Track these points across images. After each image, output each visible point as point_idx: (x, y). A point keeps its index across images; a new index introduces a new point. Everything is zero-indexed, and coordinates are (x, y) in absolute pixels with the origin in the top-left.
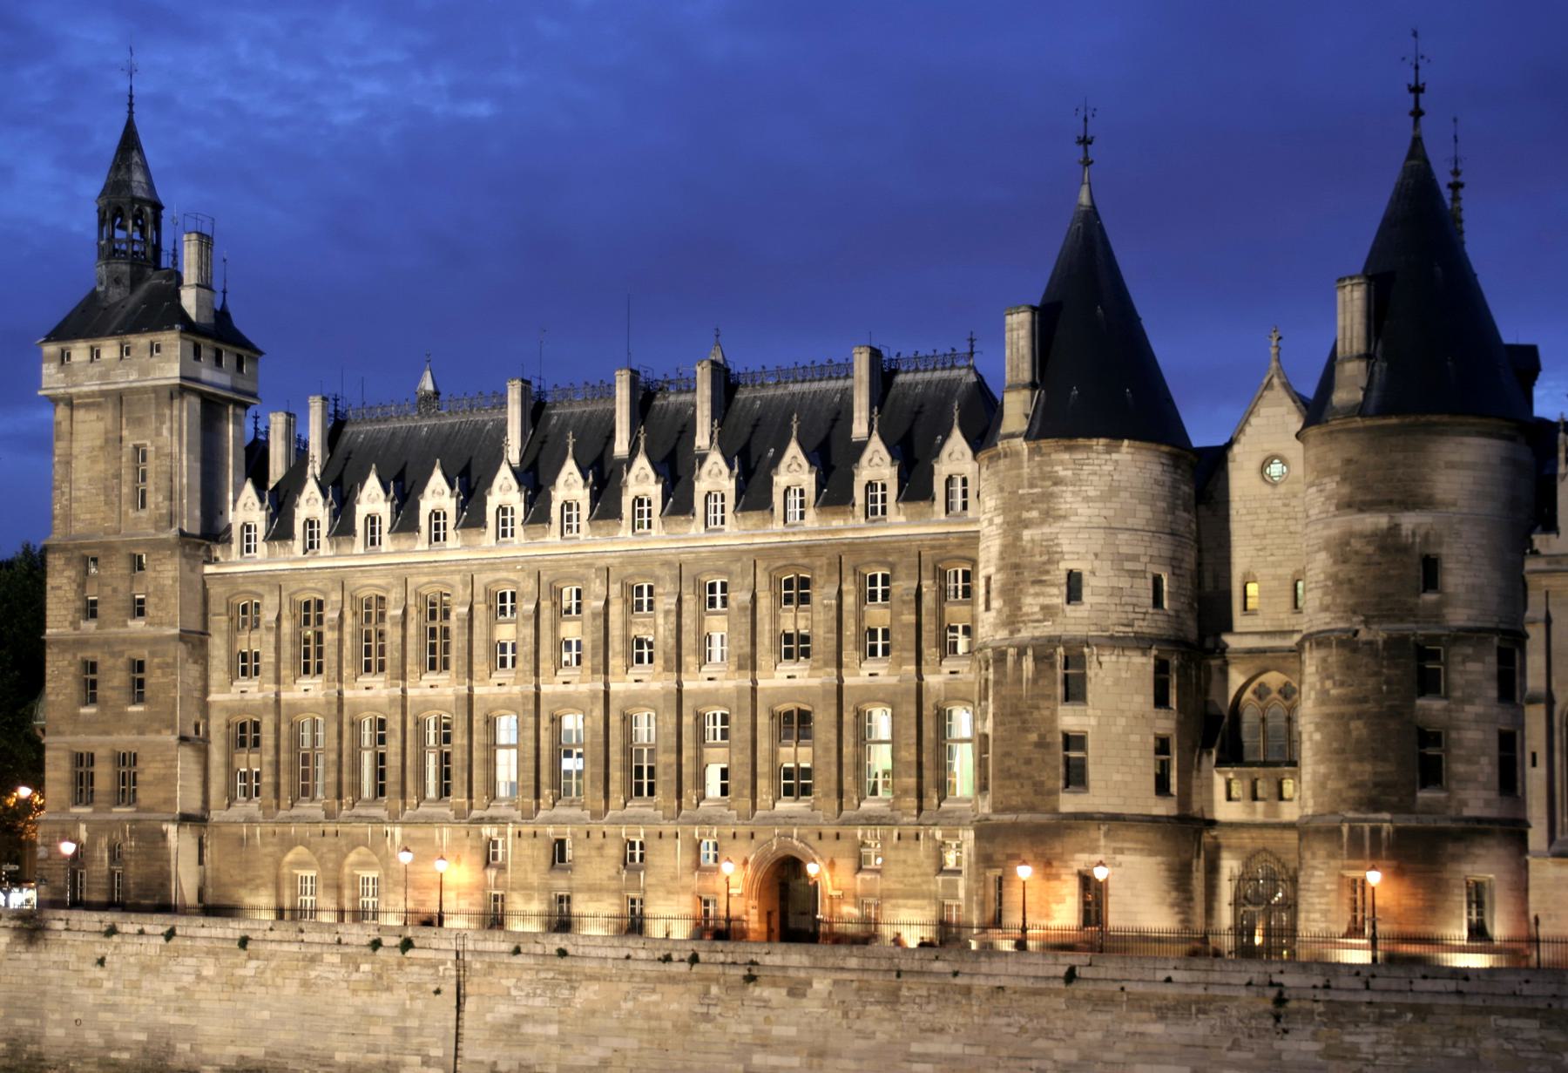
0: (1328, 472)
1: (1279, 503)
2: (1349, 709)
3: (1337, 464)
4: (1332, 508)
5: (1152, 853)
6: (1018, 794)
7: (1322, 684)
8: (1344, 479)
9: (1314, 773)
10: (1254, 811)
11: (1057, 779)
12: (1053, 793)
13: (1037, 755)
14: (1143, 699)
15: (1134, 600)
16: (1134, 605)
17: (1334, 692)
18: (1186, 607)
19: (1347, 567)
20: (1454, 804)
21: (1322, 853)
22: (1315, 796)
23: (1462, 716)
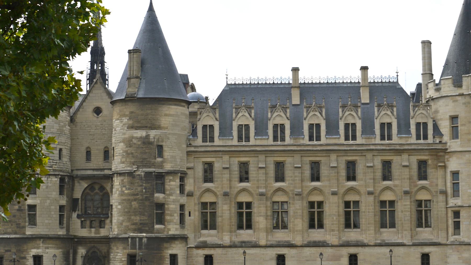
0: (124, 115)
1: (99, 124)
2: (132, 198)
3: (127, 113)
4: (126, 128)
5: (58, 248)
6: (10, 228)
7: (122, 189)
8: (130, 119)
9: (118, 219)
10: (91, 232)
11: (25, 222)
12: (24, 227)
13: (18, 214)
14: (55, 194)
15: (53, 158)
16: (53, 160)
17: (126, 192)
18: (69, 160)
19: (131, 149)
20: (166, 230)
21: (121, 248)
22: (118, 228)
23: (169, 200)
